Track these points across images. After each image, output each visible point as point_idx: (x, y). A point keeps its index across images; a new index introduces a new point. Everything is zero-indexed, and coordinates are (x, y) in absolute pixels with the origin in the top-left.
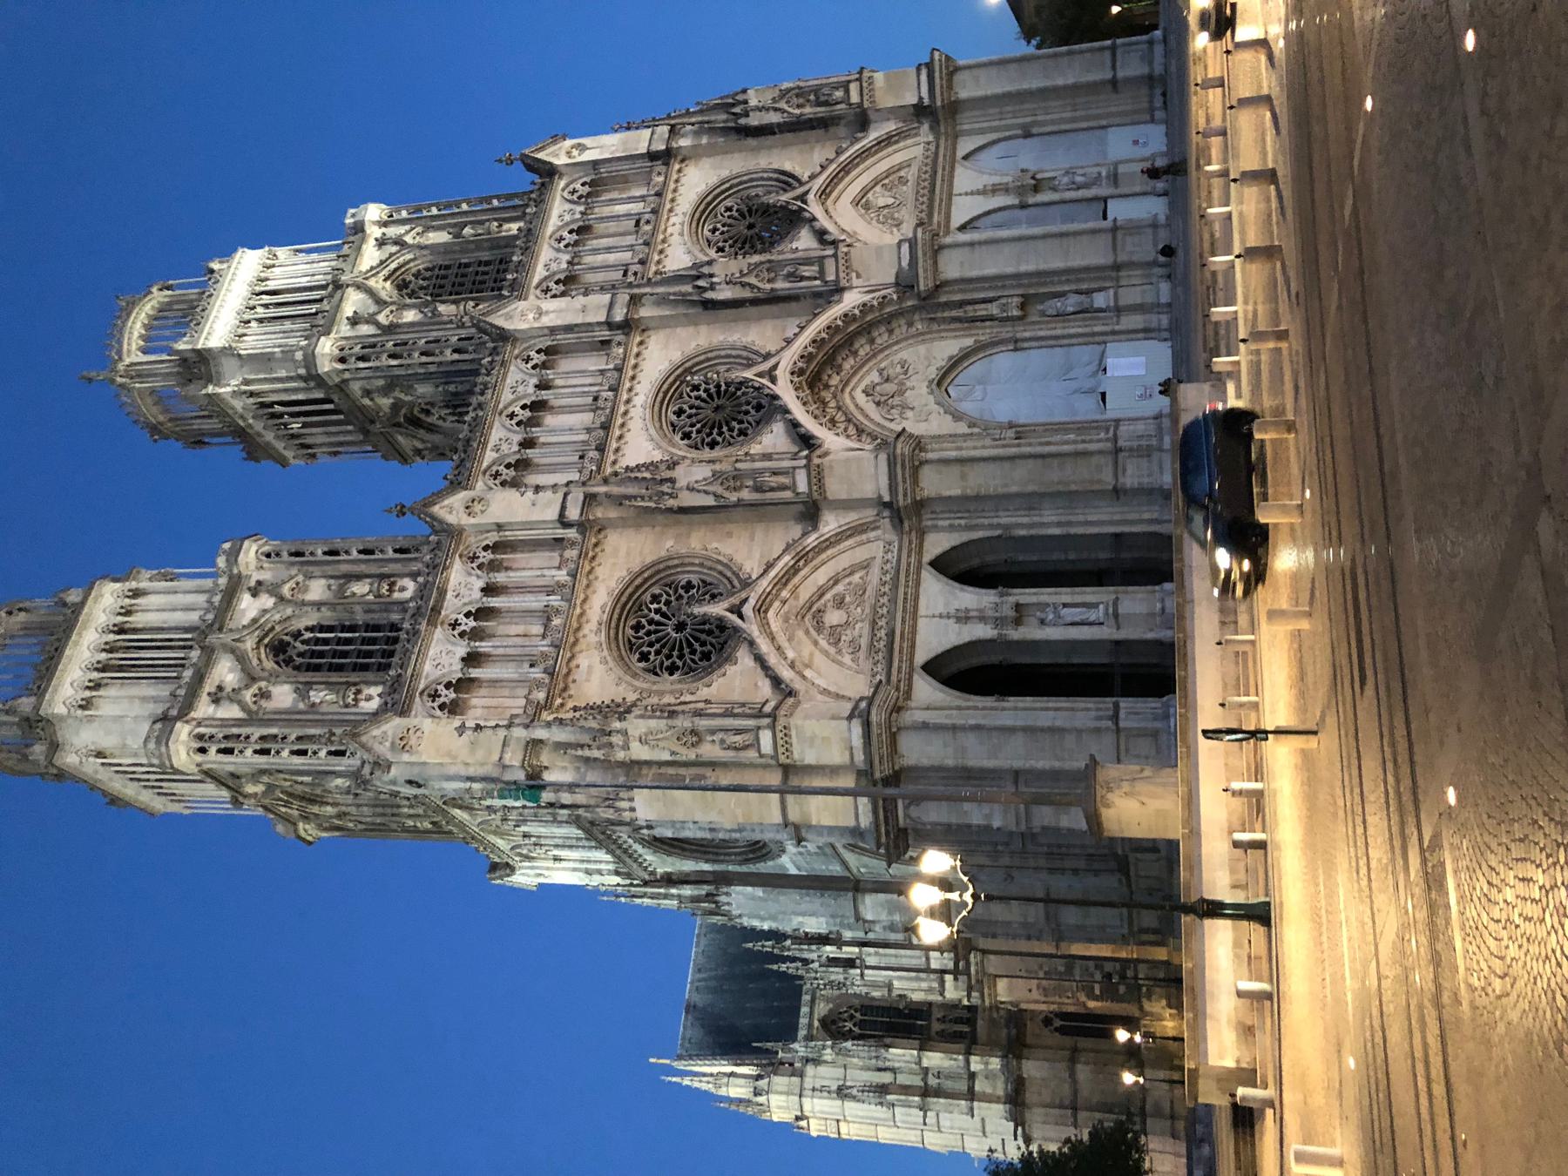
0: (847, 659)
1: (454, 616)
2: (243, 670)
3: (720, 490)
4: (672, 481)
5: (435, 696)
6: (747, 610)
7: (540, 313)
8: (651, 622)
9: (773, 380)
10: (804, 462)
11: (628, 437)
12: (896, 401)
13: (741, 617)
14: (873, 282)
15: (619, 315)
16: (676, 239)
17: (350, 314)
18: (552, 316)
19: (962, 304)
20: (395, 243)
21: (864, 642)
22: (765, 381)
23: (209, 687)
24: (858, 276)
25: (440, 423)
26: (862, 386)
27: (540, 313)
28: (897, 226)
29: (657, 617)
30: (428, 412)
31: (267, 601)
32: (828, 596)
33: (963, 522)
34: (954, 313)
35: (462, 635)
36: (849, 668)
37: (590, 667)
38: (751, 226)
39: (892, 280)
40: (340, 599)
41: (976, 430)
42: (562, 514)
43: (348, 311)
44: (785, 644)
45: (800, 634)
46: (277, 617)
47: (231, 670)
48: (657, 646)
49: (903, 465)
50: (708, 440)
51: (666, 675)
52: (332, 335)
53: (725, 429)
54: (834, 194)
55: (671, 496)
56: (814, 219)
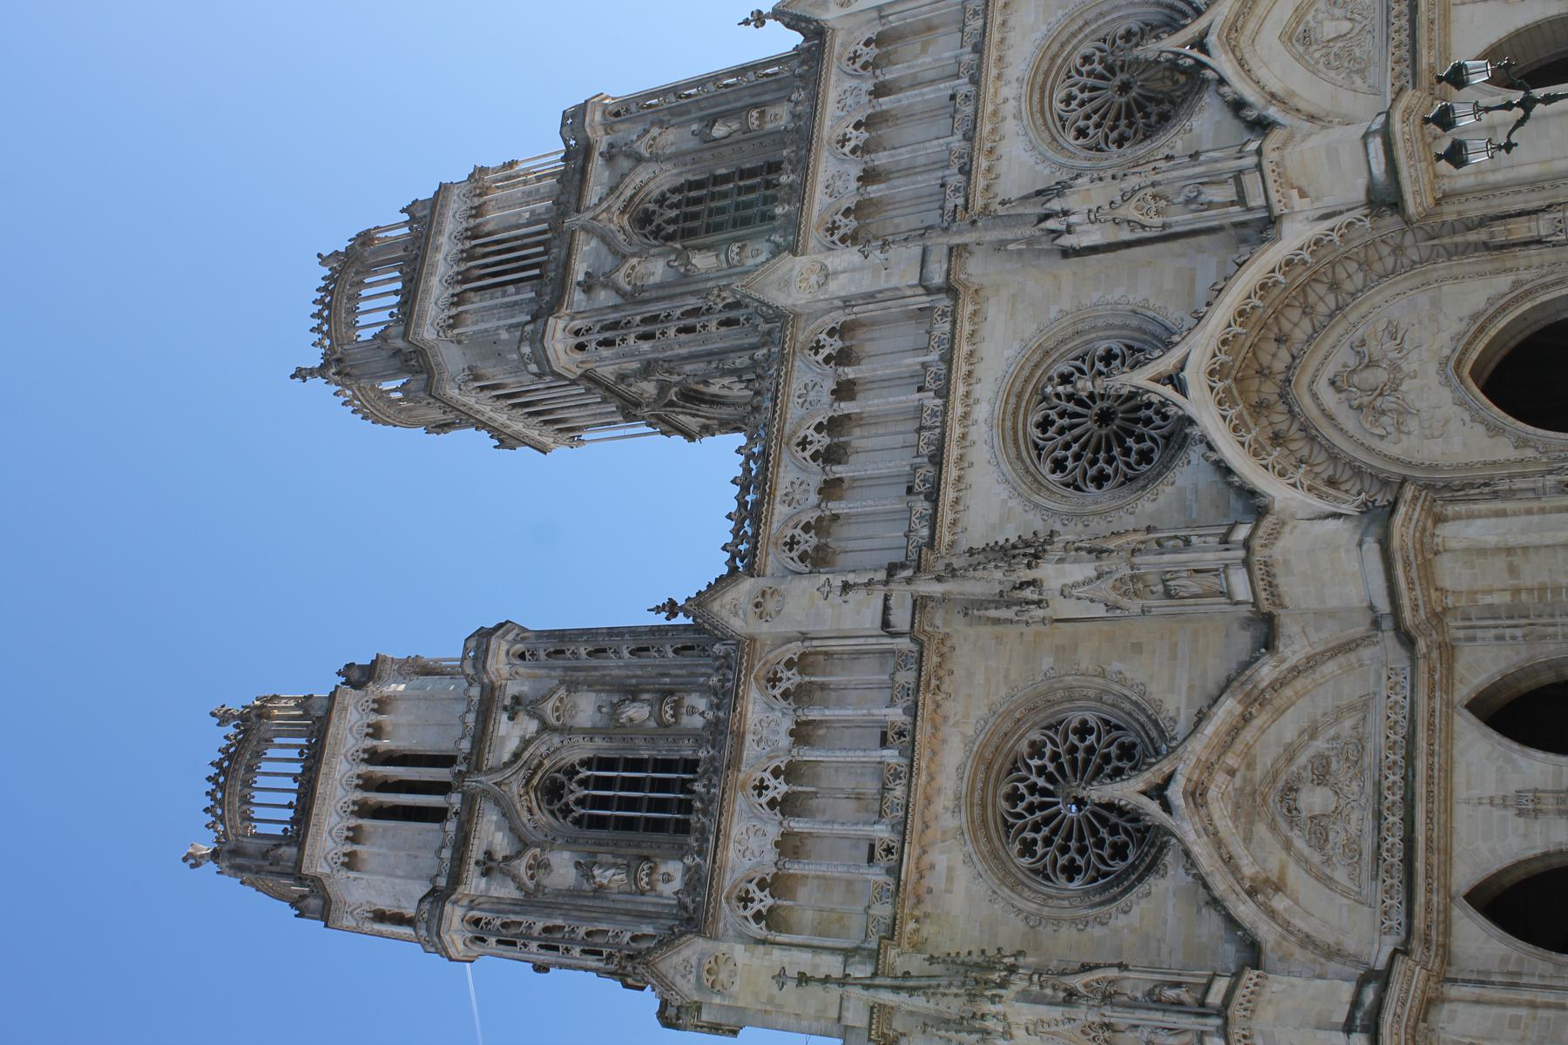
0: (1340, 875)
1: (759, 775)
2: (511, 829)
3: (1113, 597)
5: (746, 900)
6: (1175, 793)
7: (827, 275)
8: (1033, 789)
9: (1181, 388)
10: (1241, 553)
11: (972, 476)
12: (1387, 402)
13: (1167, 807)
15: (937, 279)
16: (1010, 125)
17: (581, 277)
18: (843, 278)
19: (1484, 221)
20: (627, 156)
21: (1367, 846)
23: (476, 852)
24: (1302, 194)
25: (725, 392)
26: (1330, 370)
27: (827, 275)
28: (1360, 72)
29: (1041, 782)
30: (706, 383)
31: (532, 726)
32: (1302, 759)
33: (1519, 632)
34: (1472, 237)
35: (772, 804)
36: (1345, 893)
37: (950, 869)
38: (1124, 88)
39: (1361, 196)
40: (612, 727)
41: (1529, 453)
42: (886, 624)
43: (579, 271)
44: (1237, 848)
45: (1261, 829)
46: (543, 749)
47: (499, 829)
48: (1045, 831)
49: (1407, 563)
50: (1092, 472)
51: (1062, 880)
52: (564, 311)
53: (1116, 451)
54: (1251, 25)
55: (1039, 603)
56: (1222, 81)
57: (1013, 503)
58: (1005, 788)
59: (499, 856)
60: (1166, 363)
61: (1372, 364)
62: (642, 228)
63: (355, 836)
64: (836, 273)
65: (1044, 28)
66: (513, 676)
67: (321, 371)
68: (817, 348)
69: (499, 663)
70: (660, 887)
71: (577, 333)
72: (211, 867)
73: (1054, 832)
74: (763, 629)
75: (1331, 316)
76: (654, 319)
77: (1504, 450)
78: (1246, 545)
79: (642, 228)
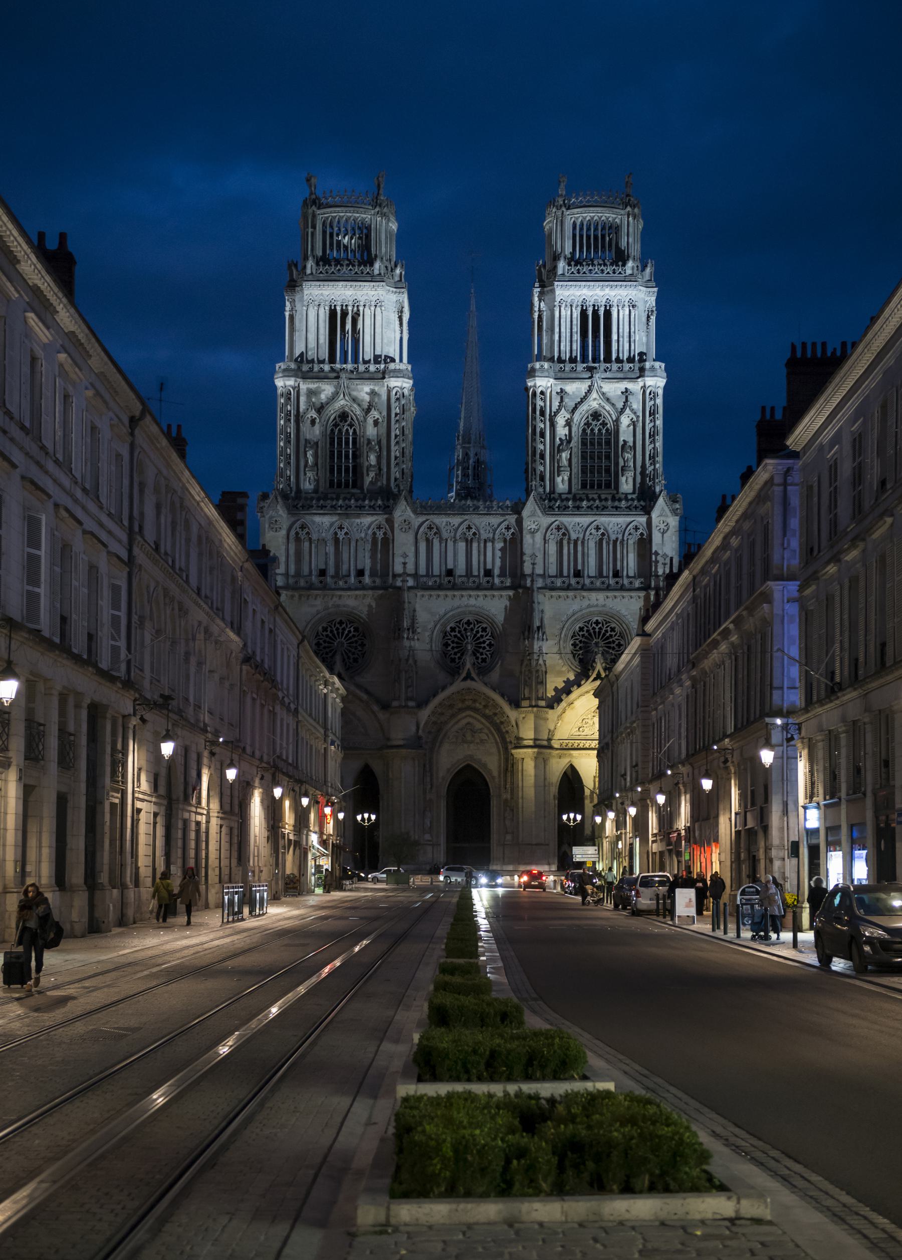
8: (344, 629)
9: (465, 679)
18: (531, 541)
22: (464, 675)
27: (533, 533)
35: (336, 534)
39: (521, 736)
56: (579, 686)
60: (474, 675)
61: (473, 736)
62: (591, 415)
64: (533, 538)
65: (626, 613)
73: (330, 638)
76: (542, 435)
77: (441, 774)
78: (406, 706)
79: (591, 415)
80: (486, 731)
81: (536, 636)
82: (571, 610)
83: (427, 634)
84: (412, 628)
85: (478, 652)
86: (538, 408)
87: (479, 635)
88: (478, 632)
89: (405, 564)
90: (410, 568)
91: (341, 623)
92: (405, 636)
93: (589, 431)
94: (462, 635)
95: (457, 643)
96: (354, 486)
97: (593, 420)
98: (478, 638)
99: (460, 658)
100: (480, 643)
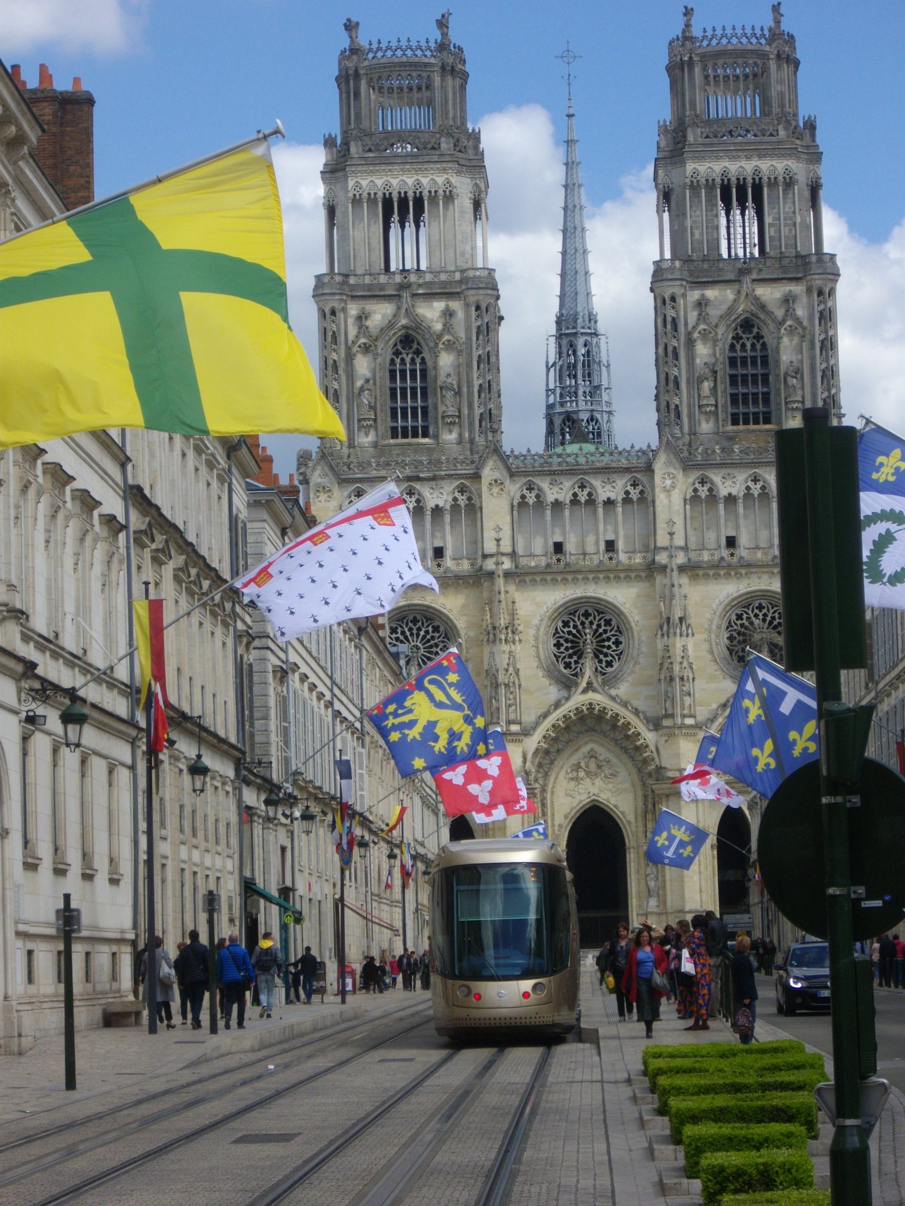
4: (494, 641)
7: (667, 491)
9: (585, 691)
12: (582, 774)
14: (662, 750)
18: (666, 501)
22: (584, 685)
23: (370, 306)
27: (667, 491)
29: (422, 633)
31: (438, 327)
34: (650, 806)
41: (556, 828)
43: (711, 293)
47: (384, 316)
50: (562, 641)
55: (488, 640)
57: (545, 609)
58: (419, 617)
59: (368, 323)
60: (595, 685)
61: (599, 767)
62: (741, 326)
63: (372, 200)
64: (669, 496)
66: (467, 305)
67: (687, 37)
68: (634, 485)
69: (473, 296)
70: (363, 430)
71: (673, 299)
72: (346, 43)
74: (485, 489)
75: (622, 748)
76: (676, 356)
80: (614, 760)
81: (678, 631)
82: (725, 593)
83: (532, 632)
84: (512, 628)
85: (601, 653)
86: (669, 319)
87: (601, 630)
88: (599, 626)
89: (498, 540)
90: (506, 547)
91: (415, 621)
92: (503, 637)
93: (738, 347)
94: (578, 631)
95: (572, 642)
96: (425, 435)
97: (744, 333)
98: (601, 634)
99: (576, 662)
100: (604, 641)
